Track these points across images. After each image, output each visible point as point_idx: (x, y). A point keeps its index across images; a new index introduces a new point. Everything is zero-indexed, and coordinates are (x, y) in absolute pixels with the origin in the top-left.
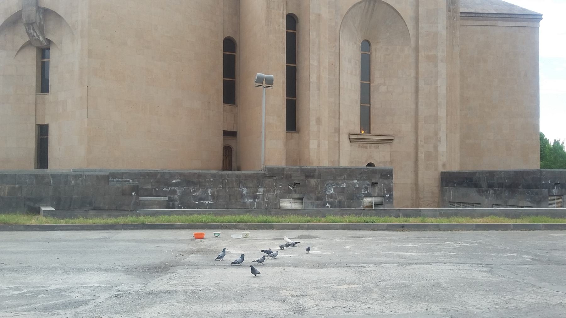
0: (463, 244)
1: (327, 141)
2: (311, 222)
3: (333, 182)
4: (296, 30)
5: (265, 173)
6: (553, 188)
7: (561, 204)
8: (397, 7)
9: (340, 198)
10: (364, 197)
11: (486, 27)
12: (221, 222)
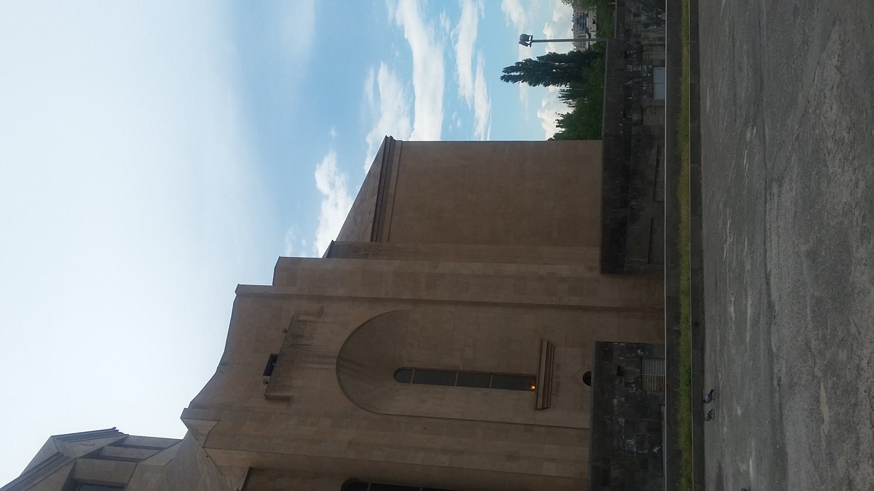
0: (728, 230)
2: (691, 477)
8: (353, 327)
10: (642, 389)
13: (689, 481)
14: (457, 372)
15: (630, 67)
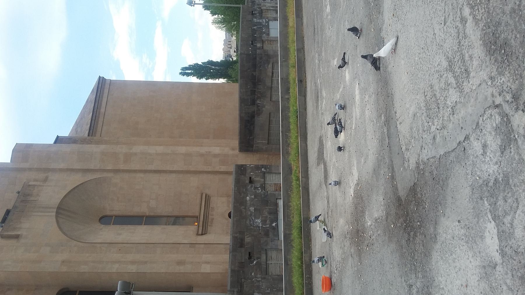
1: (204, 255)
3: (248, 220)
4: (76, 291)
5: (237, 291)
6: (256, 46)
8: (69, 188)
9: (267, 213)
10: (265, 191)
12: (303, 287)
13: (298, 179)
15: (255, 20)
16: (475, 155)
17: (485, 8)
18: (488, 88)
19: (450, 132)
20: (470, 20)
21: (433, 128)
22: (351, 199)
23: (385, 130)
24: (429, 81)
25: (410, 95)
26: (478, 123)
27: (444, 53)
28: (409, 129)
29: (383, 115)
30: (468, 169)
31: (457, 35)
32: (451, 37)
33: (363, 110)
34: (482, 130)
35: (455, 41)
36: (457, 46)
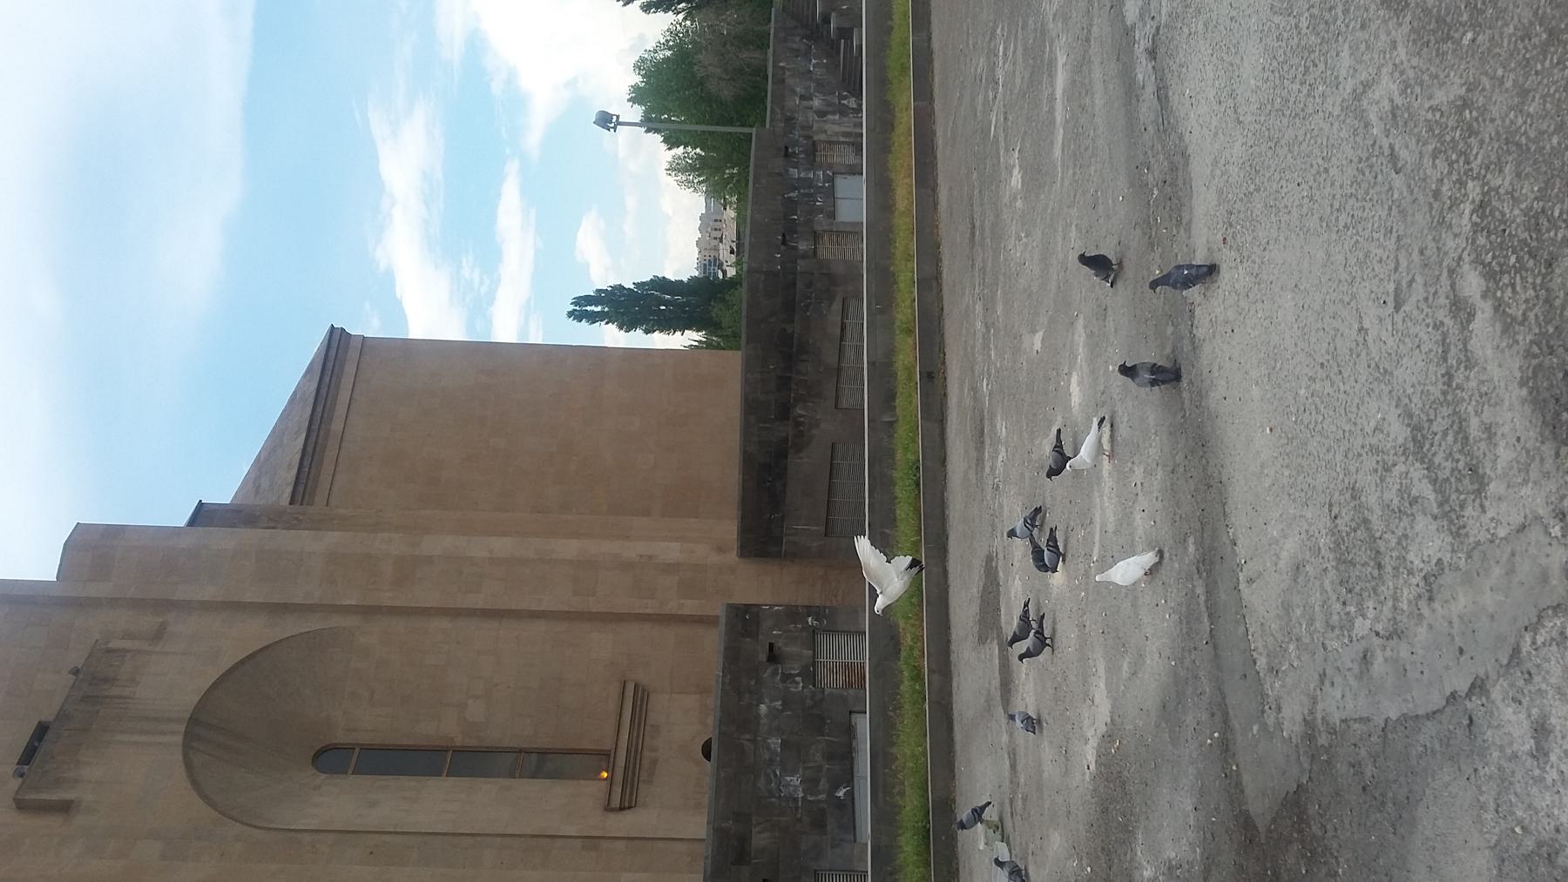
6: (795, 248)
7: (838, 236)
8: (226, 662)
10: (814, 686)
11: (340, 460)
14: (449, 751)
15: (794, 172)
16: (1509, 751)
17: (1538, 288)
18: (1550, 544)
19: (1421, 652)
20: (1483, 313)
21: (1361, 627)
22: (1087, 778)
23: (1200, 590)
24: (1347, 472)
25: (1283, 502)
26: (1516, 651)
27: (1396, 398)
28: (1280, 608)
29: (1191, 540)
30: (1484, 789)
31: (1440, 352)
32: (1421, 351)
33: (1127, 510)
34: (1530, 674)
35: (1432, 368)
36: (1440, 386)
